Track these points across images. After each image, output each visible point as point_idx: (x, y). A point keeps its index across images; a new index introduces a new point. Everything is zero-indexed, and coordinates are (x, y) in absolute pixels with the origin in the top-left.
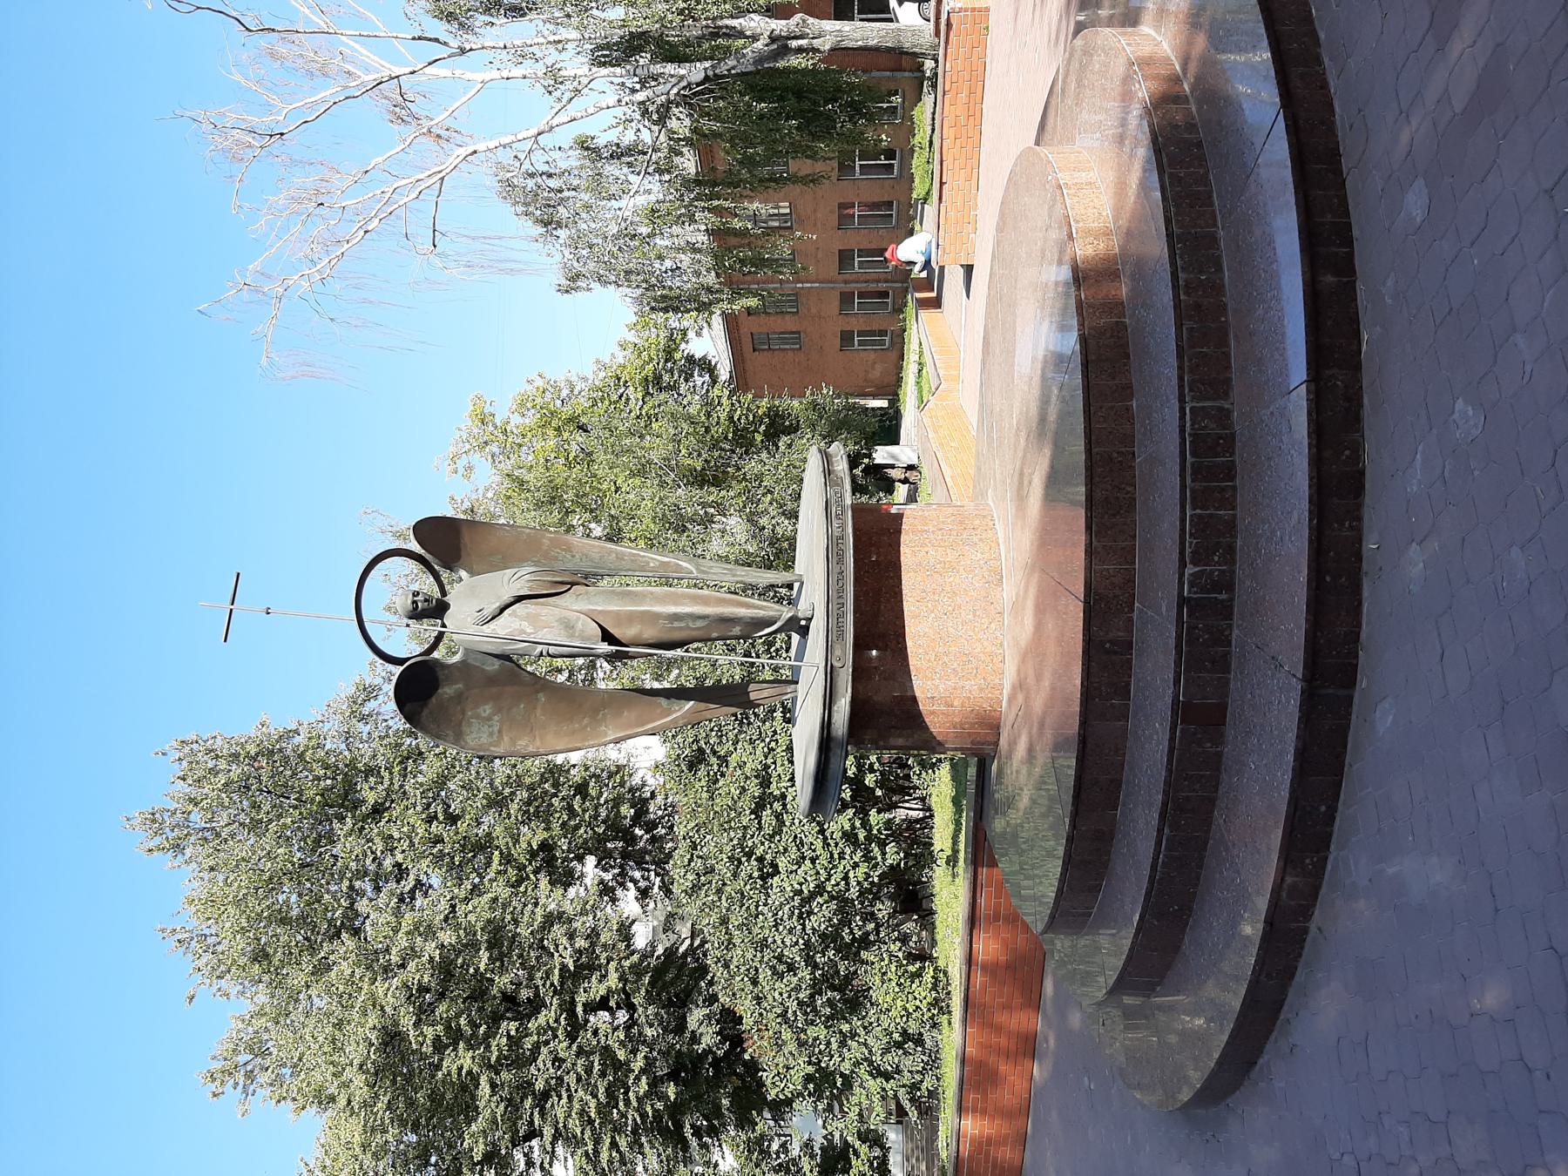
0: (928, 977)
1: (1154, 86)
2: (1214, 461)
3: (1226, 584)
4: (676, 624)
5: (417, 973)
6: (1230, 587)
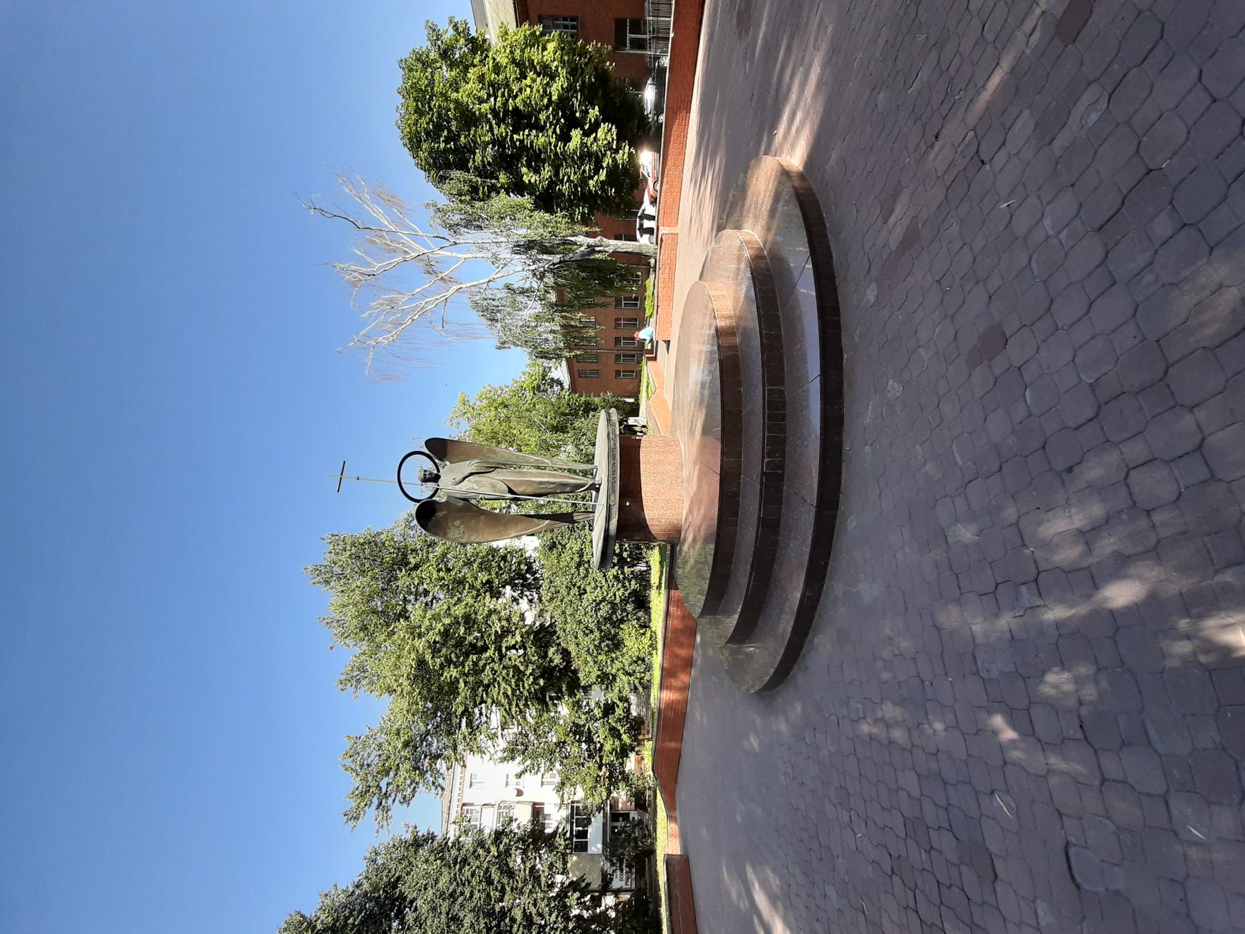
0: (648, 635)
1: (752, 252)
2: (779, 412)
3: (782, 466)
5: (433, 636)
6: (782, 467)
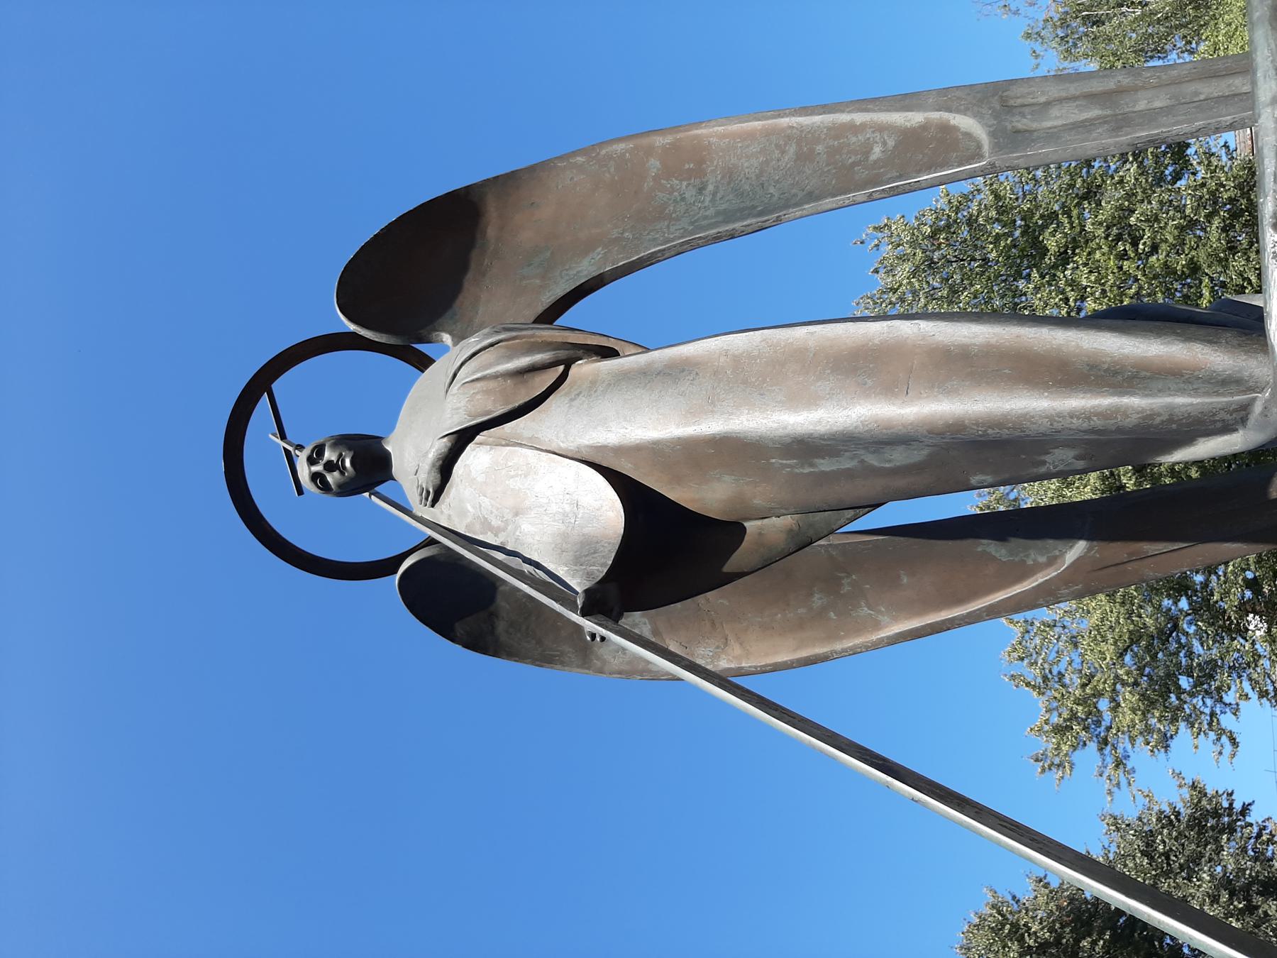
4: (825, 465)
